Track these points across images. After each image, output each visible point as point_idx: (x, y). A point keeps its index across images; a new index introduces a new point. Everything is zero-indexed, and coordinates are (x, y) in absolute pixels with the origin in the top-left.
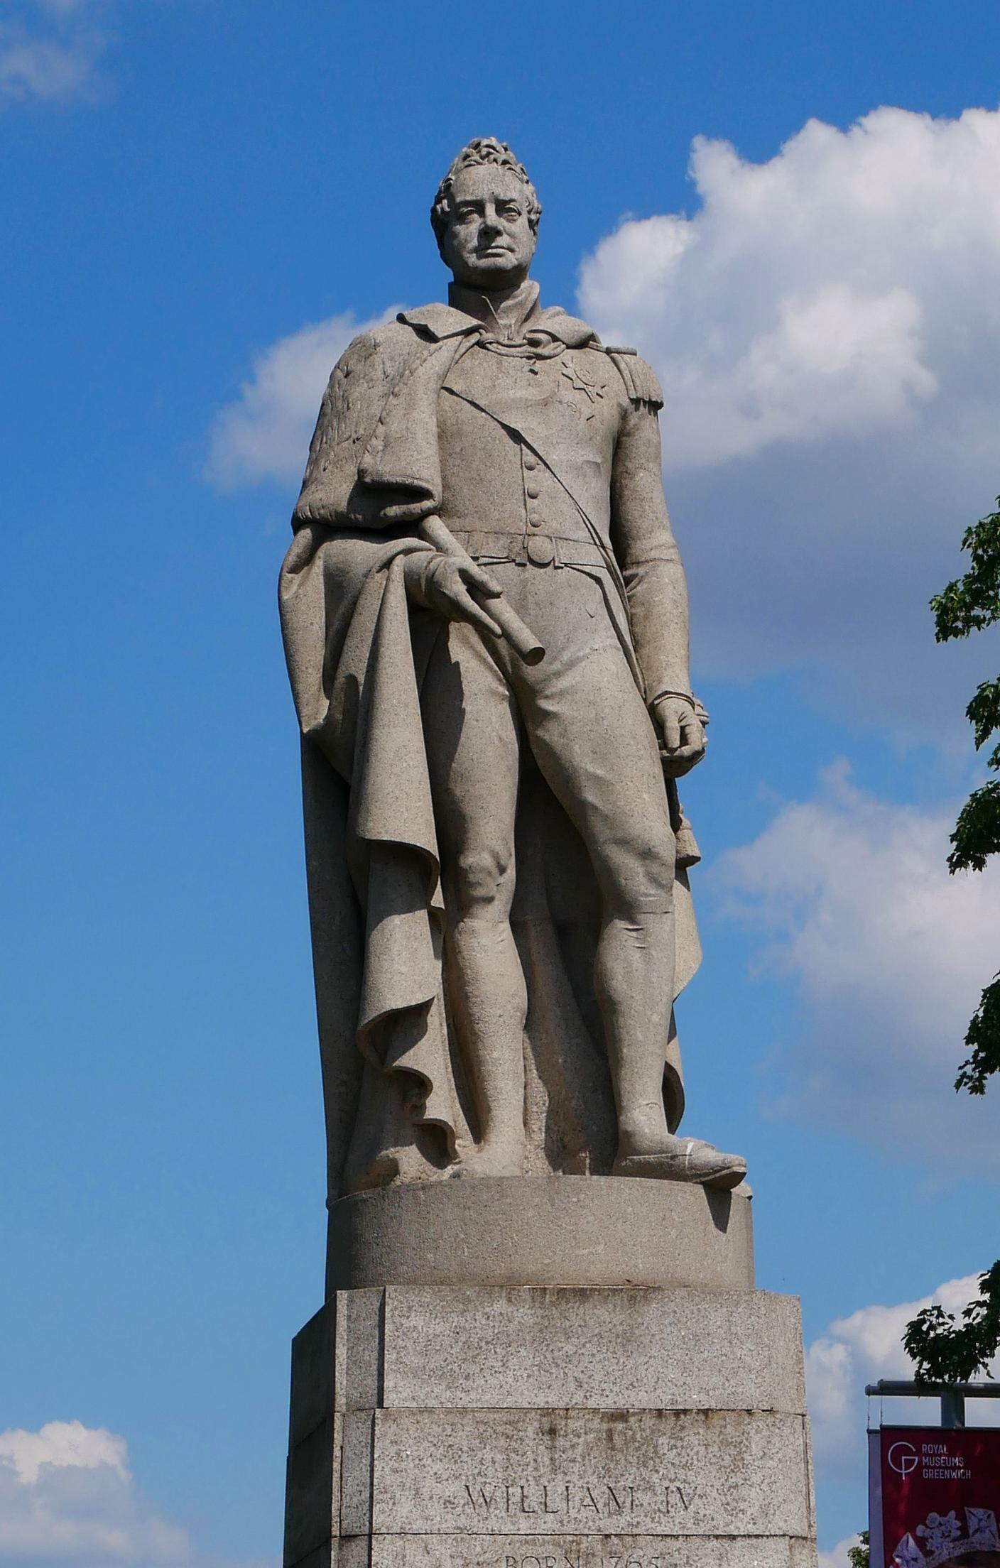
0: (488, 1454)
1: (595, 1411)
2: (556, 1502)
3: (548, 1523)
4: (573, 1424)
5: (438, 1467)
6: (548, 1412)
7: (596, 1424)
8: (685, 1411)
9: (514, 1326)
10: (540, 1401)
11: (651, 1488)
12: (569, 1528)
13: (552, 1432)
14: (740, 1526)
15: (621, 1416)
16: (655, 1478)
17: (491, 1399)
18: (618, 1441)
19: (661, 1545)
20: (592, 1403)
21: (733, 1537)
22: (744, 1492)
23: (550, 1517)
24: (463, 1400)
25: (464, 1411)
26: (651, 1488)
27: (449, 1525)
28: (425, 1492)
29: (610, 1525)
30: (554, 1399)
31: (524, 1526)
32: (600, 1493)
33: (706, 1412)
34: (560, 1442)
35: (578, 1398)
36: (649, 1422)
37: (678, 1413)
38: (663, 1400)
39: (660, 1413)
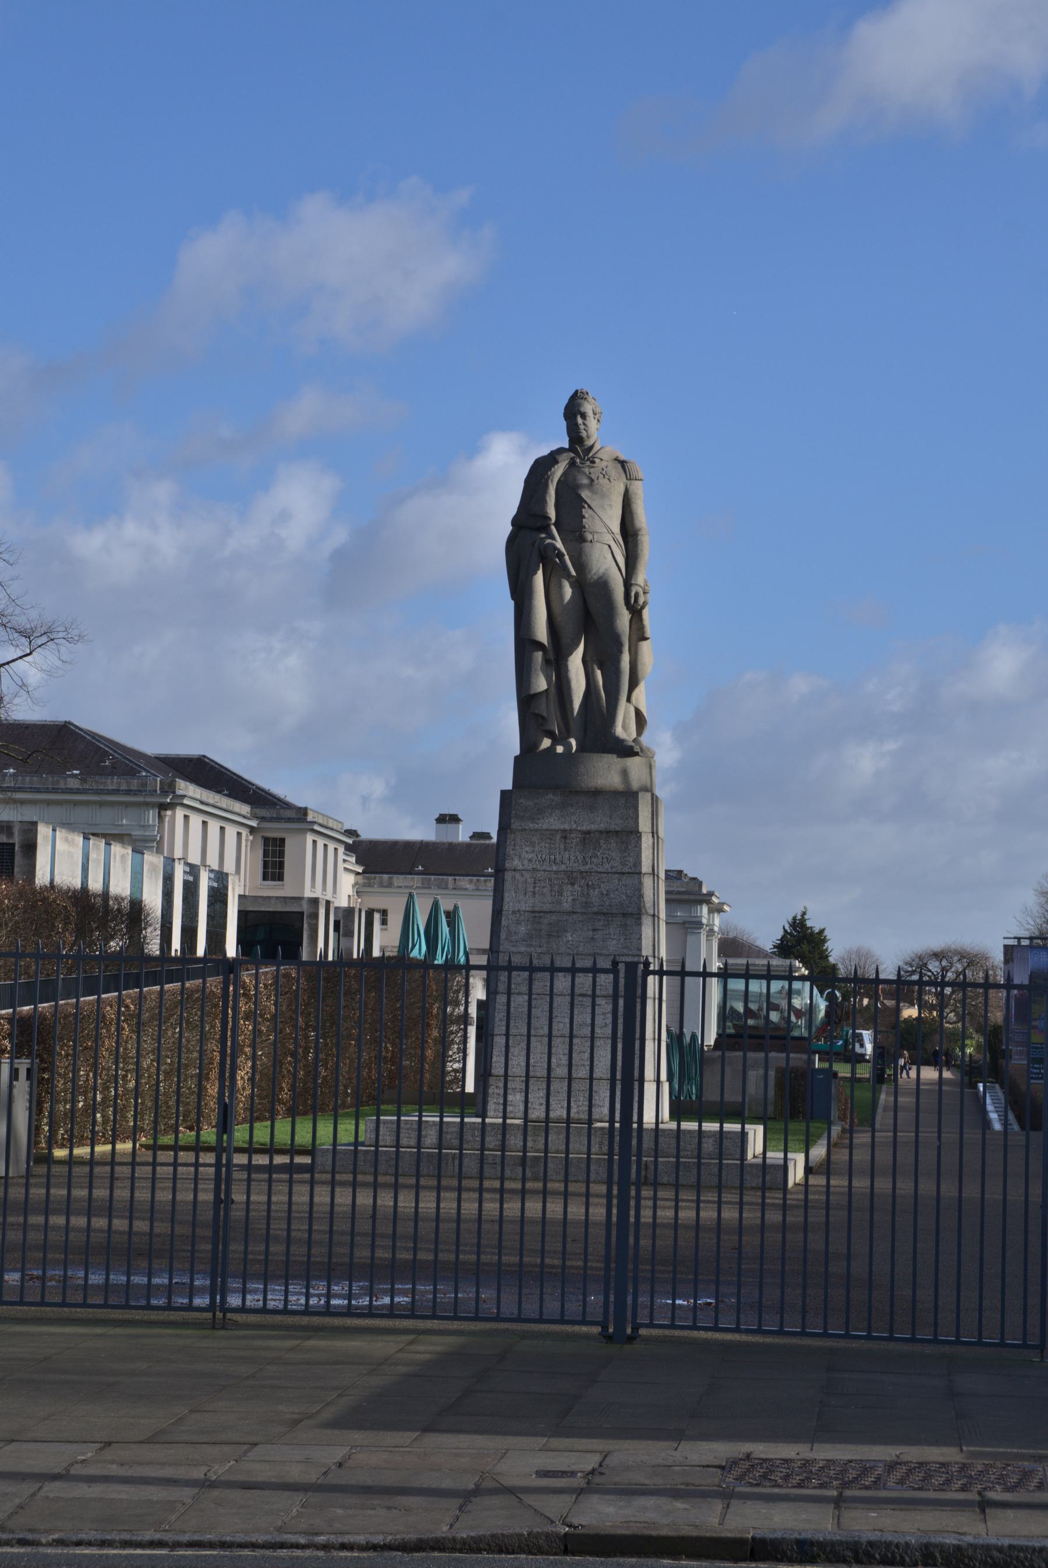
0: (543, 844)
1: (580, 831)
2: (566, 861)
3: (563, 867)
4: (572, 835)
5: (527, 849)
6: (564, 831)
7: (580, 835)
8: (610, 832)
9: (554, 803)
10: (562, 827)
11: (596, 856)
12: (569, 869)
13: (565, 838)
14: (626, 870)
15: (588, 832)
16: (599, 854)
17: (545, 827)
18: (587, 841)
19: (599, 875)
20: (579, 828)
21: (623, 873)
22: (628, 858)
23: (563, 866)
24: (536, 826)
25: (536, 830)
26: (596, 856)
27: (530, 868)
28: (522, 856)
29: (582, 868)
30: (566, 827)
31: (554, 868)
32: (580, 858)
33: (617, 832)
34: (568, 841)
35: (574, 826)
36: (597, 835)
37: (607, 832)
38: (602, 827)
39: (601, 832)
